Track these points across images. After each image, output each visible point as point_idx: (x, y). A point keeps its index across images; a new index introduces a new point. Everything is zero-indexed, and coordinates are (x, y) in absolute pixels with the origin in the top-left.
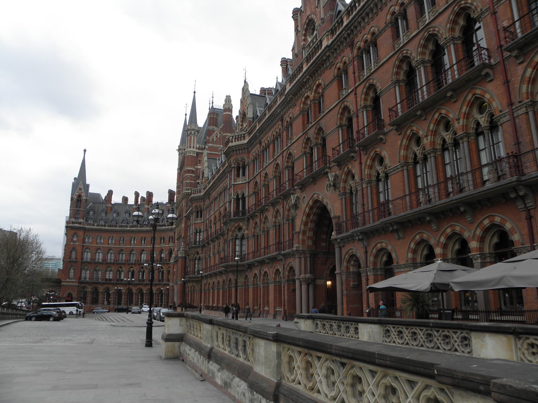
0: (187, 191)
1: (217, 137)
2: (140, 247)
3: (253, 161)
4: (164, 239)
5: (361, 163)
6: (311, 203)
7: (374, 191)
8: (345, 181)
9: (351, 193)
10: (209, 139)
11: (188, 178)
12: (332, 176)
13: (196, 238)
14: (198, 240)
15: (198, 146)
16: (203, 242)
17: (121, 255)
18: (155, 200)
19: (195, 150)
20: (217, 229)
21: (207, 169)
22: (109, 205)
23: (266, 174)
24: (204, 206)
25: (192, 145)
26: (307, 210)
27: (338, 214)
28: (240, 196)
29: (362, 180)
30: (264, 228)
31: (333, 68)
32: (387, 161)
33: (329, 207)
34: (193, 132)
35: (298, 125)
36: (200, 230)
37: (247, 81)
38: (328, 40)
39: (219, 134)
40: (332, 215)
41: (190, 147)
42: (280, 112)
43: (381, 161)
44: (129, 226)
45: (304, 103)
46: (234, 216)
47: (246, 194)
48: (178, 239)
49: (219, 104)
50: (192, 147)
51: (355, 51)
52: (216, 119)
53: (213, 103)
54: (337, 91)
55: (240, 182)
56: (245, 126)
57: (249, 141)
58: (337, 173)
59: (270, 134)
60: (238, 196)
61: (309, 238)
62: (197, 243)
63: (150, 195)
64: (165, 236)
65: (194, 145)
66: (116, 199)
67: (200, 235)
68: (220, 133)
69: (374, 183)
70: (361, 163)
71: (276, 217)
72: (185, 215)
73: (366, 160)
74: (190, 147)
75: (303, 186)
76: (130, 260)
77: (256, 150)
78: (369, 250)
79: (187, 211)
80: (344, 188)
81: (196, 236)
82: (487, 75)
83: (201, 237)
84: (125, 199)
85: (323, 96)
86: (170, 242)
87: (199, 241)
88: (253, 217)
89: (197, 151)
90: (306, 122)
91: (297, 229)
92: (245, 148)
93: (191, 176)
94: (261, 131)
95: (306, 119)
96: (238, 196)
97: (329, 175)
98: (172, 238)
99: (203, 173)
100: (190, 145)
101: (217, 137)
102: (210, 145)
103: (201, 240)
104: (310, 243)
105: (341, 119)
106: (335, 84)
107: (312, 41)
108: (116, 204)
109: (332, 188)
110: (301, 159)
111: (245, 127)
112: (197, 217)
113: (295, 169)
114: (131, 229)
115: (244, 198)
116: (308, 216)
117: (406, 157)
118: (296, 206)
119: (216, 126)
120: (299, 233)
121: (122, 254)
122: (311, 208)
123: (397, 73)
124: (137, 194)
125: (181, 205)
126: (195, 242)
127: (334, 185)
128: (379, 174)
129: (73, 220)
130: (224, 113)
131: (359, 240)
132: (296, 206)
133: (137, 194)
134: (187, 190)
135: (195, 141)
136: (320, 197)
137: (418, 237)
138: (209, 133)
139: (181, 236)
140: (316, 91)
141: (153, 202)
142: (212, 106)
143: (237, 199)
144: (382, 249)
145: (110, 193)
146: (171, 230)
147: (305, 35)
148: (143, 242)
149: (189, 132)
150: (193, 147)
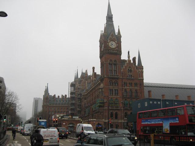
49: (84, 72)
66: (57, 96)
84: (59, 96)
118: (91, 108)
124: (62, 95)
129: (46, 103)
133: (62, 95)
145: (55, 95)
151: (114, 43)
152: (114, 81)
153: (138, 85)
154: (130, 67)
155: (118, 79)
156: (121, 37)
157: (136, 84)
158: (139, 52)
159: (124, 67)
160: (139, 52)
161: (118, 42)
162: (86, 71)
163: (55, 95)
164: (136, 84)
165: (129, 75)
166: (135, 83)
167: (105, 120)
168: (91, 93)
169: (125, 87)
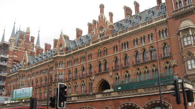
5: (121, 72)
6: (100, 79)
26: (99, 81)
29: (121, 76)
34: (13, 41)
40: (109, 84)
41: (11, 47)
49: (24, 30)
51: (121, 43)
52: (23, 36)
61: (98, 89)
70: (121, 72)
73: (123, 71)
74: (11, 47)
89: (14, 49)
102: (20, 47)
104: (98, 91)
119: (22, 39)
122: (100, 81)
123: (134, 53)
138: (19, 42)
140: (103, 49)
142: (20, 30)
147: (99, 30)
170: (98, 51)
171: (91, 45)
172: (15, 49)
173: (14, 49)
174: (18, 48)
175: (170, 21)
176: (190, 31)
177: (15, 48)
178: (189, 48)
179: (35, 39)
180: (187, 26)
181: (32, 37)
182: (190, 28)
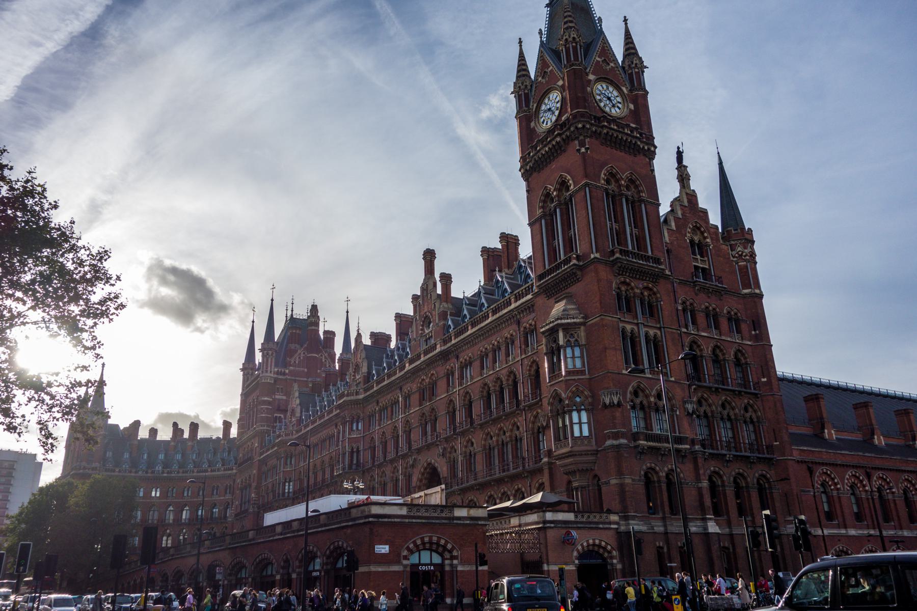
0: (262, 428)
1: (299, 358)
2: (181, 500)
3: (370, 416)
4: (217, 490)
7: (468, 462)
8: (450, 453)
9: (454, 461)
10: (290, 362)
11: (264, 411)
12: (441, 448)
13: (285, 489)
14: (287, 491)
15: (276, 370)
16: (294, 494)
17: (151, 513)
18: (201, 434)
19: (272, 375)
20: (318, 480)
21: (299, 407)
22: (136, 442)
23: (384, 432)
24: (295, 450)
25: (269, 368)
26: (422, 470)
27: (445, 475)
28: (355, 450)
30: (381, 482)
31: (444, 367)
32: (475, 445)
33: (439, 470)
35: (415, 398)
36: (290, 479)
37: (360, 332)
38: (441, 346)
39: (302, 355)
40: (441, 476)
41: (267, 372)
42: (399, 383)
43: (472, 444)
44: (166, 471)
45: (421, 383)
46: (348, 469)
47: (362, 448)
48: (242, 490)
49: (302, 313)
50: (269, 372)
53: (292, 310)
54: (446, 385)
55: (355, 436)
56: (357, 377)
57: (364, 398)
58: (445, 446)
59: (389, 397)
60: (352, 449)
62: (286, 495)
63: (194, 427)
64: (220, 485)
65: (271, 369)
67: (289, 486)
68: (304, 353)
69: (468, 457)
71: (393, 473)
72: (259, 458)
75: (419, 451)
76: (165, 519)
77: (372, 407)
78: (464, 500)
79: (261, 454)
80: (450, 457)
81: (285, 486)
82: (518, 414)
83: (291, 487)
84: (153, 432)
85: (436, 383)
86: (226, 493)
87: (289, 492)
88: (369, 470)
89: (276, 376)
90: (422, 398)
91: (414, 484)
92: (360, 404)
93: (267, 408)
94: (379, 392)
95: (422, 396)
96: (352, 449)
97: (440, 447)
98: (230, 487)
99: (293, 410)
100: (267, 368)
101: (299, 358)
103: (291, 490)
105: (448, 408)
106: (445, 380)
107: (428, 333)
108: (142, 439)
109: (441, 457)
110: (418, 429)
111: (358, 379)
112: (286, 464)
113: (412, 435)
114: (169, 475)
115: (358, 452)
116: (423, 474)
117: (485, 446)
120: (415, 487)
121: (154, 511)
122: (425, 469)
125: (249, 443)
126: (284, 493)
127: (443, 455)
128: (471, 452)
130: (310, 328)
131: (458, 494)
132: (413, 466)
134: (262, 426)
135: (273, 364)
136: (433, 461)
137: (489, 493)
139: (250, 486)
140: (430, 378)
141: (199, 437)
142: (292, 315)
143: (352, 452)
144: (472, 500)
146: (229, 476)
148: (185, 495)
149: (265, 352)
150: (271, 372)
151: (615, 93)
152: (638, 286)
153: (744, 326)
154: (697, 228)
155: (657, 277)
156: (641, 67)
157: (735, 321)
158: (721, 164)
159: (673, 224)
160: (721, 164)
161: (631, 91)
162: (314, 309)
163: (137, 424)
164: (735, 321)
165: (696, 267)
166: (729, 312)
167: (626, 518)
168: (414, 386)
169: (687, 327)
170: (421, 383)
171: (408, 367)
172: (280, 377)
173: (276, 376)
174: (287, 371)
175: (540, 301)
176: (561, 335)
177: (277, 373)
178: (557, 381)
179: (336, 339)
180: (553, 322)
181: (325, 332)
182: (558, 325)
